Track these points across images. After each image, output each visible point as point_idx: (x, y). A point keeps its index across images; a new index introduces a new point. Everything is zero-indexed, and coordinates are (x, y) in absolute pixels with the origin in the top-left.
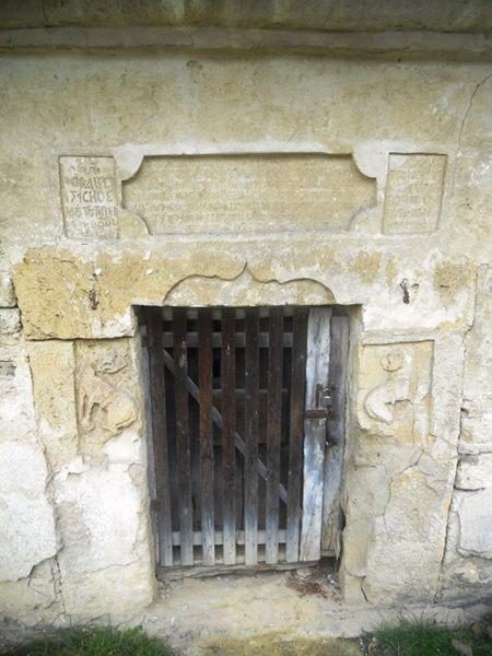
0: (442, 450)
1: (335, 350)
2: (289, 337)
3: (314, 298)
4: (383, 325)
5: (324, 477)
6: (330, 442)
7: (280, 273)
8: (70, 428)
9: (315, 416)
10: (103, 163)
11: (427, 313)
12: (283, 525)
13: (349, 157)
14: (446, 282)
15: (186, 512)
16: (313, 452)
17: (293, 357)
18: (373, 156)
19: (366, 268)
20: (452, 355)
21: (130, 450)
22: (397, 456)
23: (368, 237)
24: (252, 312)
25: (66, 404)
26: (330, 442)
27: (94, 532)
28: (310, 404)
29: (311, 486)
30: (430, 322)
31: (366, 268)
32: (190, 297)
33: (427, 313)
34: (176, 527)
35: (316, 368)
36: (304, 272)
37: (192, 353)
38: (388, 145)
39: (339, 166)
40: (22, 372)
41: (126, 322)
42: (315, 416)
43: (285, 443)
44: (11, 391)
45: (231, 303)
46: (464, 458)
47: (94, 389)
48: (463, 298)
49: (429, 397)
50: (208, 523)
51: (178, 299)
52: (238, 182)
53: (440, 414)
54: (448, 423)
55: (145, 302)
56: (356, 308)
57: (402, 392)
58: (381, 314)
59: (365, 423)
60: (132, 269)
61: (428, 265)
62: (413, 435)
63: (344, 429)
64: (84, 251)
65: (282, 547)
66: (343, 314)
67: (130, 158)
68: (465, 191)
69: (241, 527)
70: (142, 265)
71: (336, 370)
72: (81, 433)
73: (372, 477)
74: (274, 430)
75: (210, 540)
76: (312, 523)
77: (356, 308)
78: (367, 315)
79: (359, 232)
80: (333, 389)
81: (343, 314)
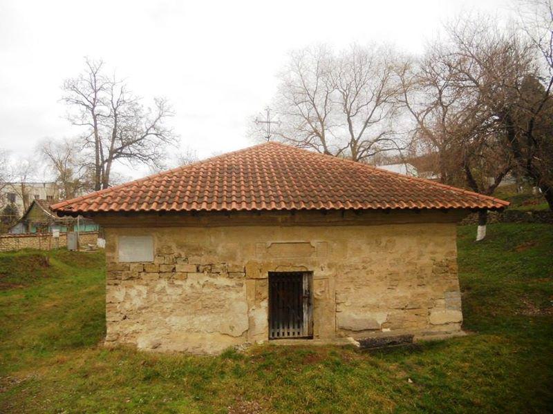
0: (332, 302)
1: (309, 282)
2: (299, 280)
3: (304, 270)
4: (318, 275)
5: (308, 313)
6: (309, 304)
7: (297, 265)
8: (253, 298)
9: (305, 297)
10: (264, 244)
11: (326, 273)
12: (299, 327)
13: (309, 243)
14: (330, 266)
15: (276, 322)
16: (305, 306)
17: (300, 284)
18: (314, 243)
19: (314, 264)
20: (332, 281)
21: (265, 304)
22: (323, 304)
23: (314, 258)
24: (291, 273)
25: (253, 293)
26: (309, 304)
27: (257, 324)
28: (304, 295)
29: (305, 316)
30: (327, 275)
31: (314, 264)
33: (326, 273)
34: (273, 328)
35: (305, 286)
36: (302, 265)
37: (278, 283)
38: (316, 241)
39: (307, 244)
40: (244, 287)
41: (267, 275)
42: (305, 297)
43: (299, 303)
44: (242, 290)
45: (288, 271)
46: (338, 304)
47: (259, 290)
48: (334, 269)
49: (328, 290)
50: (281, 326)
51: (277, 270)
52: (288, 248)
53: (331, 294)
54: (333, 296)
55: (271, 271)
56: (312, 272)
57: (323, 289)
58: (317, 273)
59: (316, 297)
60: (268, 265)
61: (326, 263)
62: (326, 299)
63: (312, 301)
64: (259, 261)
65: (299, 333)
66: (310, 273)
67: (269, 243)
68: (332, 249)
69: (289, 328)
70: (270, 263)
71: (309, 287)
72: (256, 299)
73: (318, 310)
74: (296, 301)
75: (281, 331)
76: (306, 326)
77: (312, 272)
78: (314, 274)
79: (312, 257)
80: (309, 291)
81: (310, 273)
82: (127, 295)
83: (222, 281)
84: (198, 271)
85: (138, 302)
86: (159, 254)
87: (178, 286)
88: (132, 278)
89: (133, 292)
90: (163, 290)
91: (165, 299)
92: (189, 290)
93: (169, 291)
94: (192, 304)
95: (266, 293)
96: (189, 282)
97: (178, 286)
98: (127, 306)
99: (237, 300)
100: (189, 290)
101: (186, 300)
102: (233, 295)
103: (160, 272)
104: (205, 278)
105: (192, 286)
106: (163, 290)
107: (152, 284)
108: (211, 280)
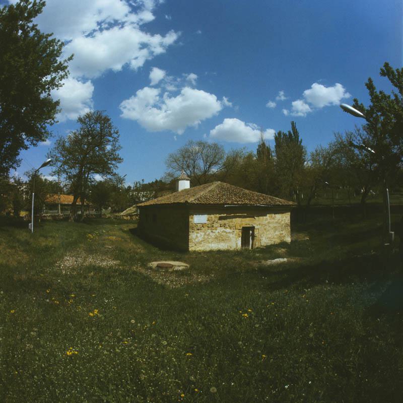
14: (259, 224)
21: (240, 238)
32: (245, 226)
82: (197, 236)
83: (228, 230)
84: (221, 227)
85: (200, 239)
86: (208, 220)
87: (214, 232)
88: (198, 230)
89: (199, 235)
90: (209, 235)
91: (209, 237)
92: (217, 234)
93: (211, 234)
94: (219, 239)
95: (241, 234)
96: (218, 231)
97: (214, 232)
98: (197, 240)
99: (233, 237)
100: (217, 234)
101: (216, 238)
102: (231, 236)
103: (208, 227)
104: (223, 229)
105: (219, 232)
106: (209, 235)
107: (205, 231)
108: (225, 230)
